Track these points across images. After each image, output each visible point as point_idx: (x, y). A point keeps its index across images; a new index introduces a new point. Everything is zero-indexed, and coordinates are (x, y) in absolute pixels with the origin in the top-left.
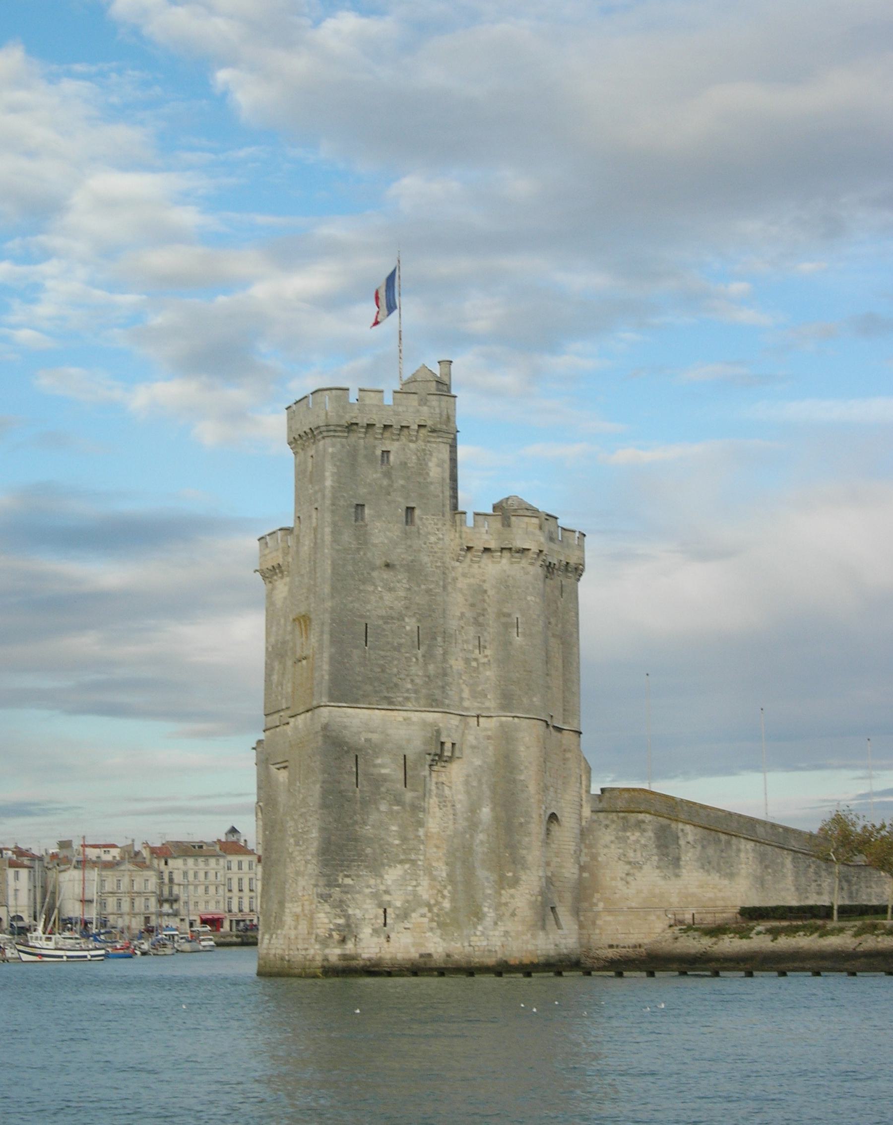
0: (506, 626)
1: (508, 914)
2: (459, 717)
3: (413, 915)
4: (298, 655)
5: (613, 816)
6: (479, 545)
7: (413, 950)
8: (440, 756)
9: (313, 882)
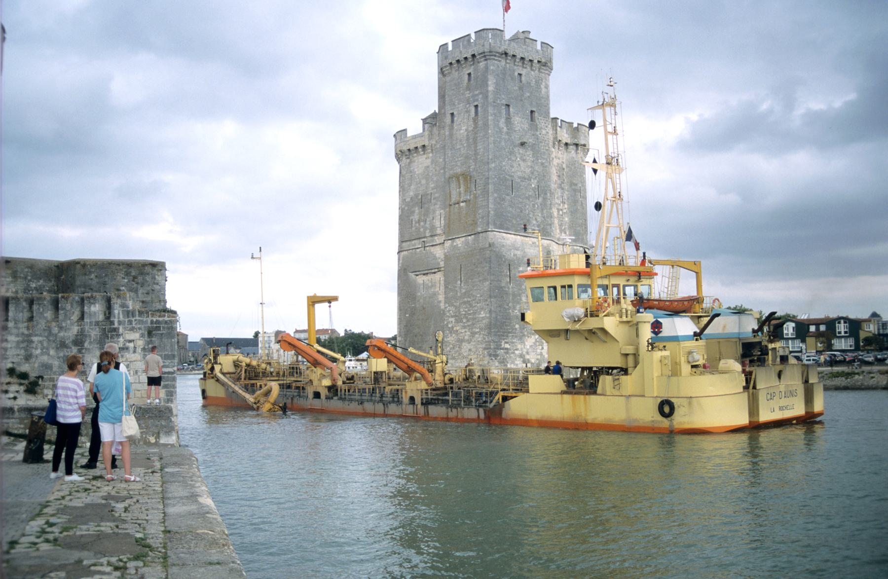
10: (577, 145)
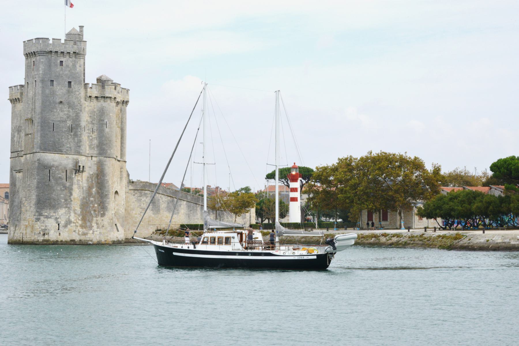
1: (101, 226)
3: (69, 226)
4: (27, 133)
5: (136, 192)
6: (94, 95)
8: (79, 170)
9: (33, 214)
10: (104, 97)
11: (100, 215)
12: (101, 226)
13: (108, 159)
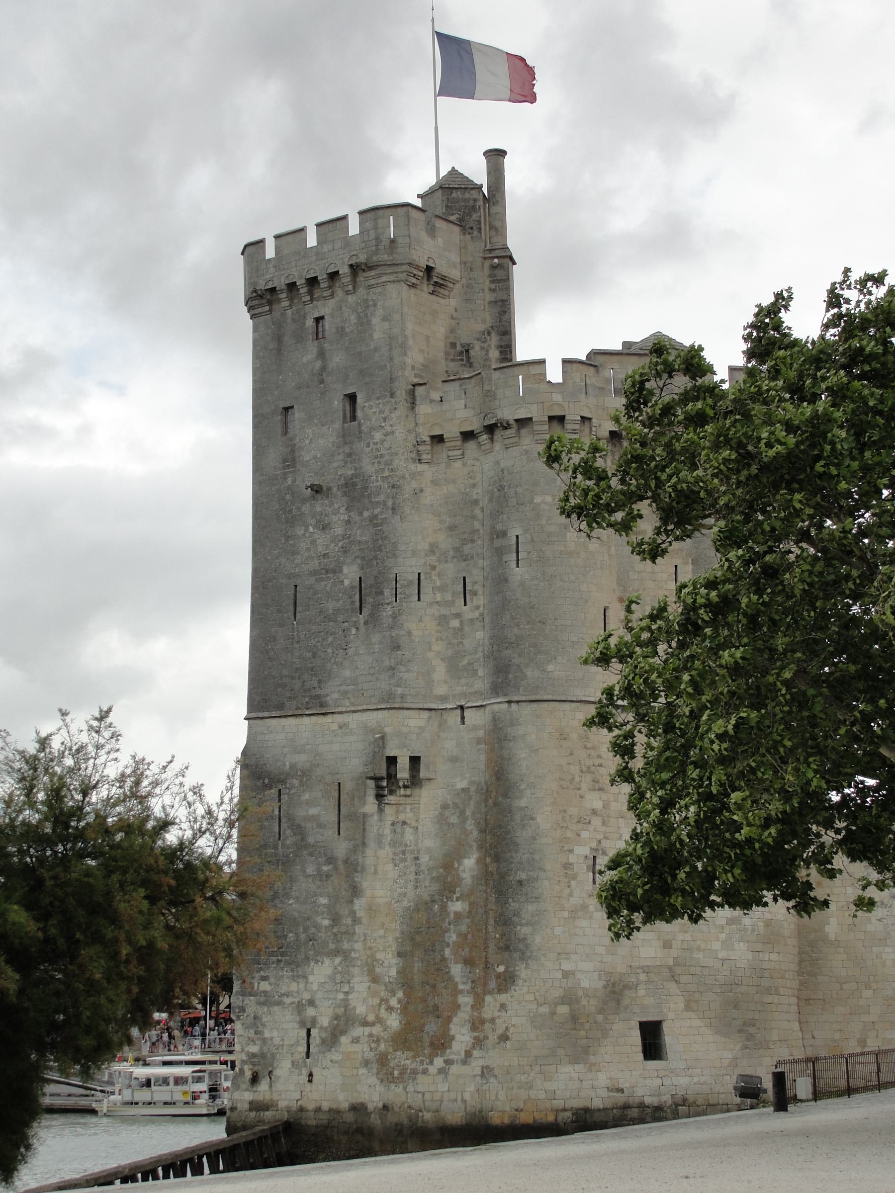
0: (500, 552)
1: (493, 1038)
2: (426, 714)
3: (344, 1039)
6: (451, 431)
7: (341, 1097)
8: (391, 776)
11: (493, 984)
12: (493, 1038)
13: (526, 710)
